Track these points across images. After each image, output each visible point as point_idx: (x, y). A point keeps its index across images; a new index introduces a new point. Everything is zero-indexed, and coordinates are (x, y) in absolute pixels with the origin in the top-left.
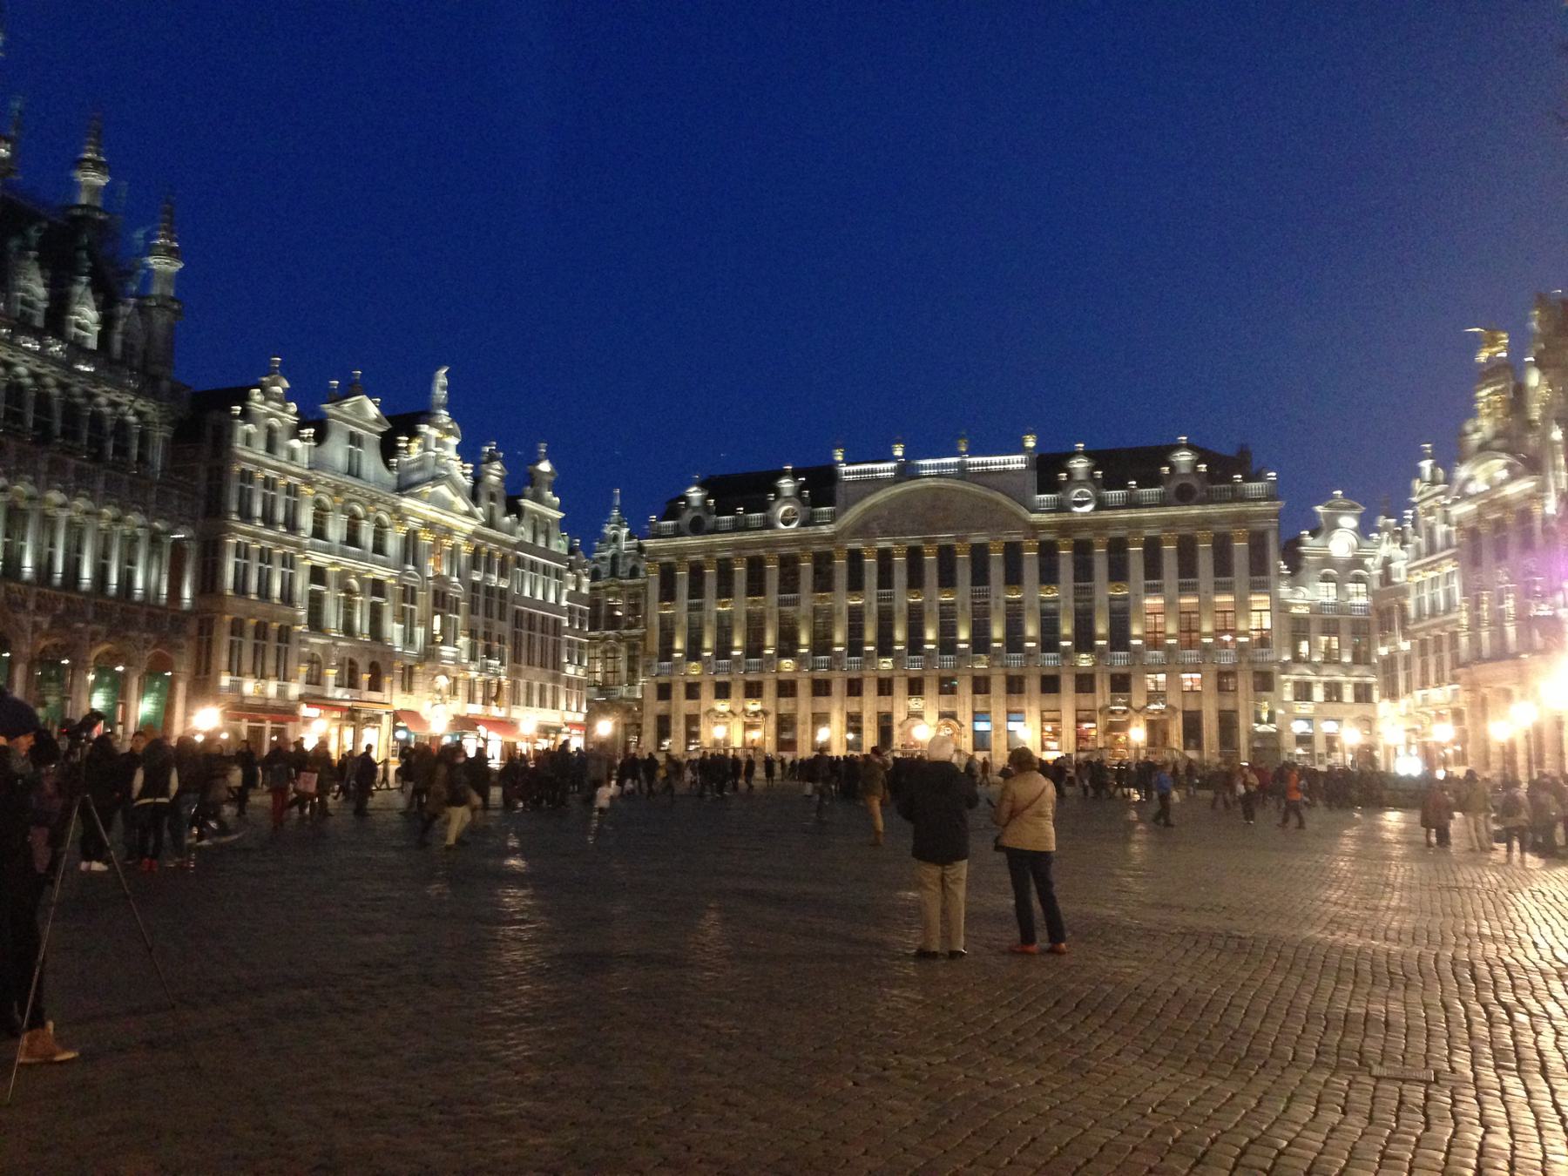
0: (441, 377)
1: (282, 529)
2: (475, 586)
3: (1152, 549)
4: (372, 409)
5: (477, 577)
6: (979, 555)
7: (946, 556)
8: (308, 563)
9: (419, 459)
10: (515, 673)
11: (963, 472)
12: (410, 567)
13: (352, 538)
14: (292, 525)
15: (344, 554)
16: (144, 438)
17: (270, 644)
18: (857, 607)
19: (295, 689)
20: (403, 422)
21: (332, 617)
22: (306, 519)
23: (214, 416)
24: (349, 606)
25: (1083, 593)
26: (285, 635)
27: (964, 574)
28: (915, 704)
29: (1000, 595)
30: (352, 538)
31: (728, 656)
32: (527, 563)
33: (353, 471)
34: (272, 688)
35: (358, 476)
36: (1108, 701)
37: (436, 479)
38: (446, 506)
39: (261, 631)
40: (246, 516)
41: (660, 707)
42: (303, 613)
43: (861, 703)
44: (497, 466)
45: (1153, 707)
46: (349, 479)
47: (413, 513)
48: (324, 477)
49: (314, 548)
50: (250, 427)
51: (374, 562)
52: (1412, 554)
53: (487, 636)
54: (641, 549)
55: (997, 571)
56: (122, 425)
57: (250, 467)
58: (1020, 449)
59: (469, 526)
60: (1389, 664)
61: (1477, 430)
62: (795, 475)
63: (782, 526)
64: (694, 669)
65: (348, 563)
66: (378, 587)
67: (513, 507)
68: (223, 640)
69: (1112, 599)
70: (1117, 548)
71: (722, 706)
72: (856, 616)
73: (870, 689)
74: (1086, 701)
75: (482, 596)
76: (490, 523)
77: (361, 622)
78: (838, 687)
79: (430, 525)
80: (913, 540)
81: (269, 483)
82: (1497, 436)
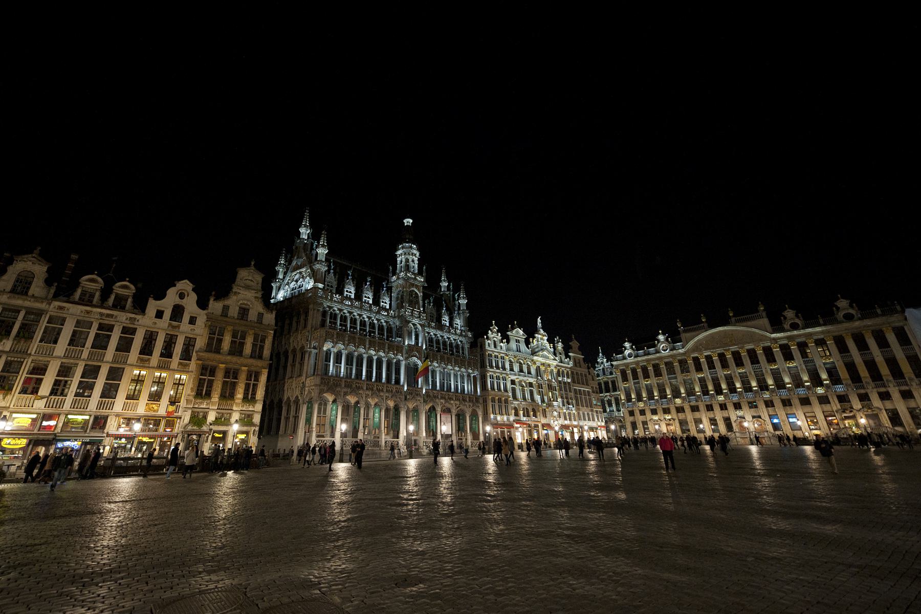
0: (539, 320)
2: (560, 382)
4: (521, 332)
5: (560, 379)
10: (578, 410)
13: (521, 370)
14: (504, 369)
16: (463, 348)
17: (503, 405)
19: (512, 418)
20: (531, 333)
21: (519, 395)
22: (507, 366)
23: (480, 340)
24: (523, 391)
26: (506, 401)
28: (740, 413)
30: (521, 370)
33: (519, 350)
34: (505, 418)
37: (542, 350)
38: (547, 358)
39: (500, 400)
40: (492, 367)
42: (510, 394)
48: (511, 353)
53: (567, 398)
54: (612, 365)
56: (457, 346)
59: (555, 363)
62: (664, 334)
64: (641, 405)
66: (531, 385)
67: (567, 356)
68: (490, 404)
71: (655, 418)
72: (702, 381)
73: (717, 408)
74: (827, 407)
77: (528, 396)
78: (702, 407)
79: (543, 364)
80: (720, 351)
81: (496, 357)
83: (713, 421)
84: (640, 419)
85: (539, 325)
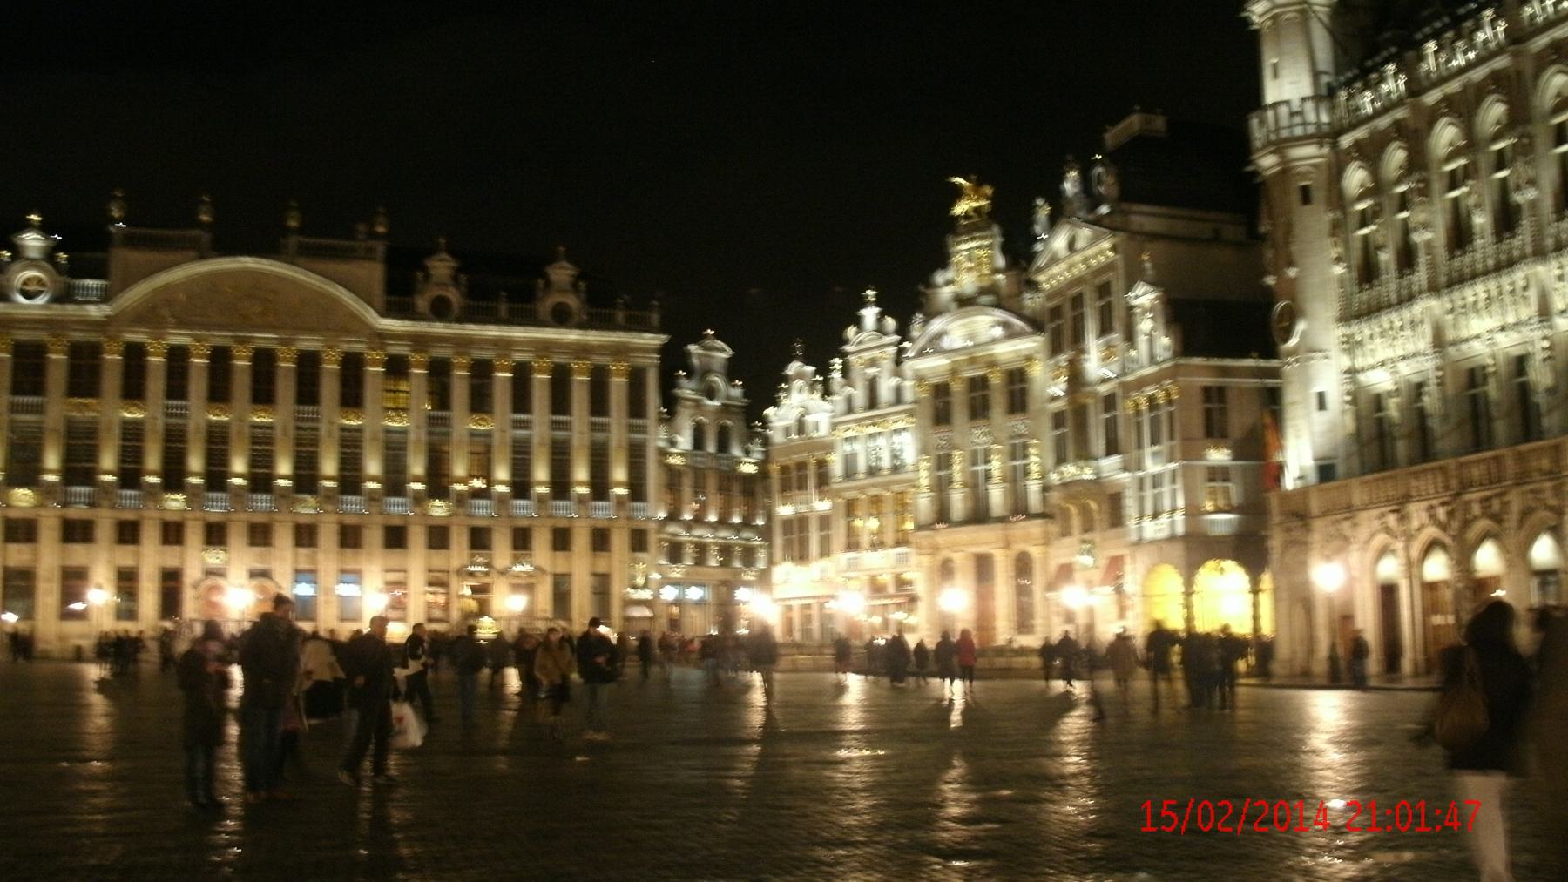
3: (522, 375)
6: (308, 365)
7: (264, 362)
18: (136, 422)
25: (438, 425)
27: (285, 388)
28: (214, 558)
29: (333, 419)
36: (466, 560)
43: (137, 555)
45: (518, 568)
52: (841, 407)
55: (329, 389)
60: (796, 528)
61: (949, 283)
62: (44, 229)
63: (21, 299)
72: (132, 436)
74: (438, 559)
80: (220, 338)
82: (983, 291)
83: (127, 581)
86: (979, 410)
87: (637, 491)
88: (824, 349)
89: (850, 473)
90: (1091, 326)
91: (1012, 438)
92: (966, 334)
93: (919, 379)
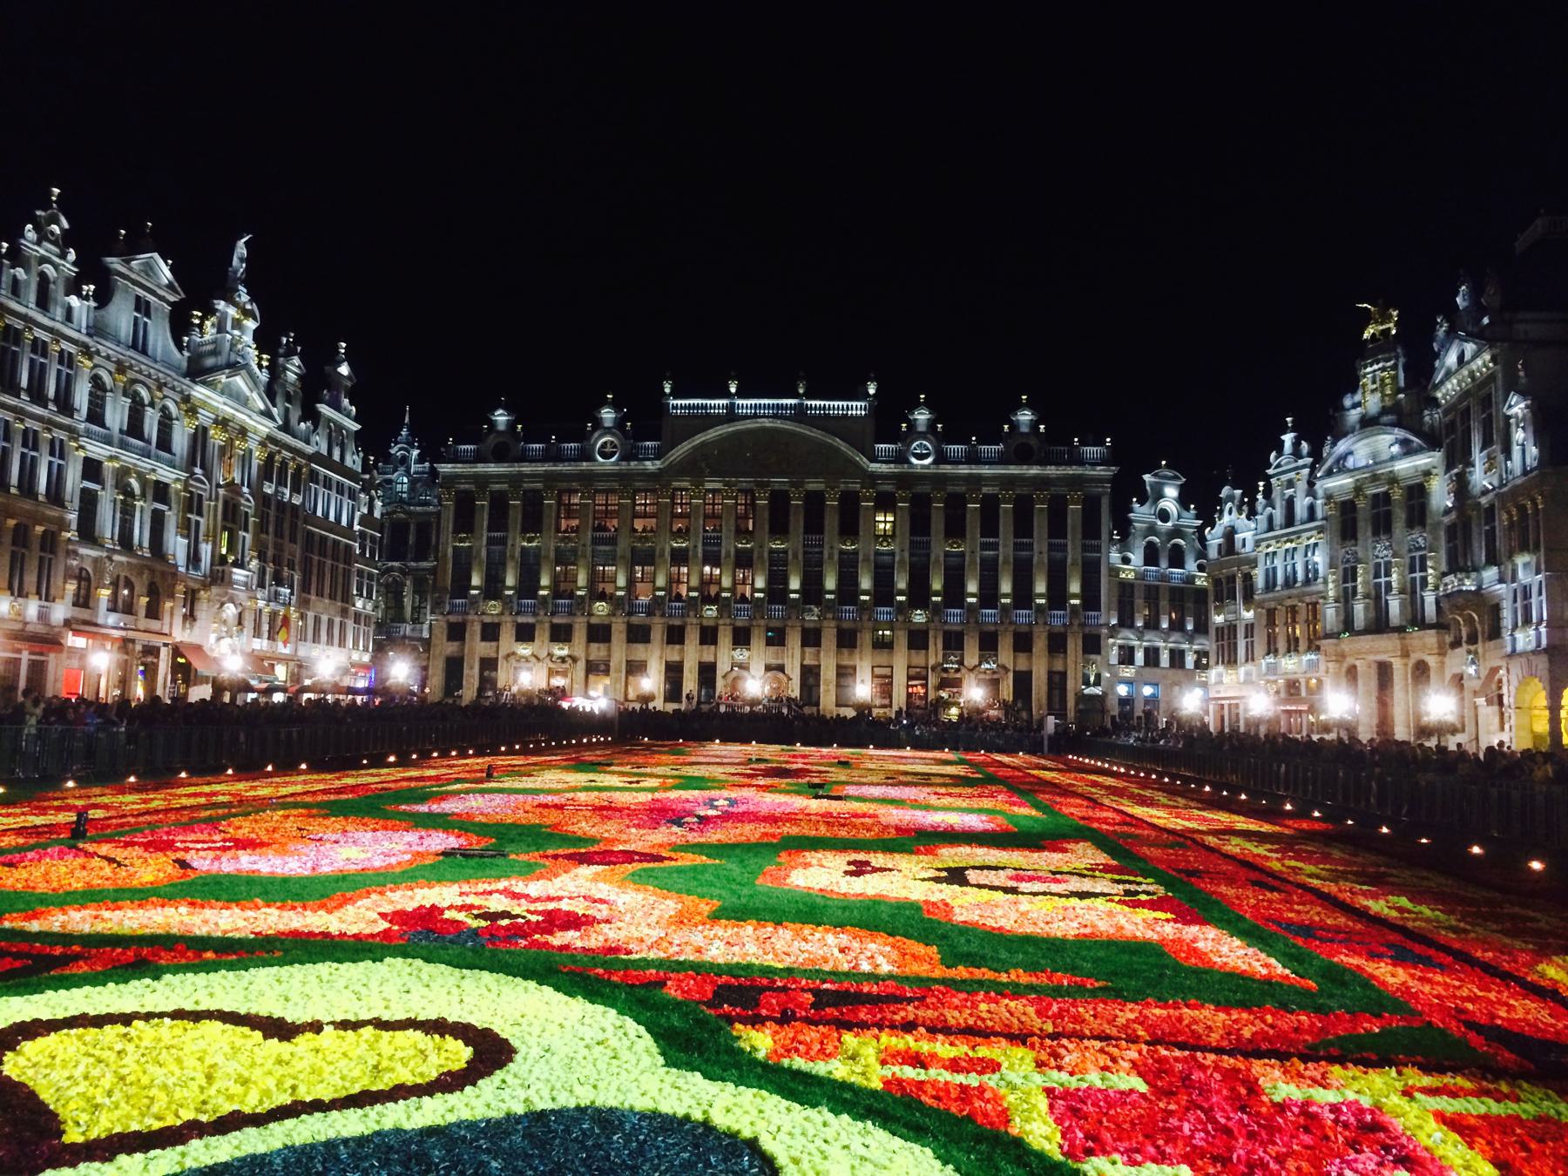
0: (241, 249)
1: (52, 407)
2: (266, 498)
3: (990, 507)
4: (165, 272)
5: (269, 489)
6: (815, 503)
8: (82, 454)
9: (214, 342)
10: (304, 604)
11: (800, 414)
12: (198, 470)
13: (135, 427)
14: (64, 403)
15: (123, 445)
19: (60, 612)
20: (200, 289)
22: (81, 396)
24: (127, 512)
26: (50, 543)
28: (740, 655)
29: (835, 546)
31: (534, 595)
32: (321, 478)
33: (139, 344)
35: (144, 352)
36: (940, 659)
37: (233, 367)
38: (243, 401)
41: (451, 648)
42: (73, 517)
43: (682, 651)
44: (296, 360)
45: (985, 666)
46: (131, 353)
47: (205, 405)
48: (107, 347)
49: (89, 434)
50: (20, 272)
51: (158, 459)
52: (1263, 525)
53: (277, 561)
54: (434, 473)
55: (831, 522)
57: (19, 324)
58: (864, 395)
59: (264, 427)
60: (1227, 635)
61: (1356, 405)
62: (616, 405)
64: (493, 608)
65: (130, 458)
66: (160, 491)
67: (311, 415)
69: (947, 554)
70: (956, 505)
71: (524, 650)
73: (692, 637)
74: (918, 659)
75: (272, 513)
76: (286, 428)
77: (141, 533)
78: (657, 634)
79: (223, 423)
81: (39, 347)
82: (1384, 411)
83: (674, 672)
84: (478, 648)
85: (238, 265)
86: (1382, 526)
87: (1091, 599)
88: (1252, 477)
89: (1270, 585)
90: (1476, 440)
91: (1410, 551)
92: (1371, 452)
93: (1329, 497)
